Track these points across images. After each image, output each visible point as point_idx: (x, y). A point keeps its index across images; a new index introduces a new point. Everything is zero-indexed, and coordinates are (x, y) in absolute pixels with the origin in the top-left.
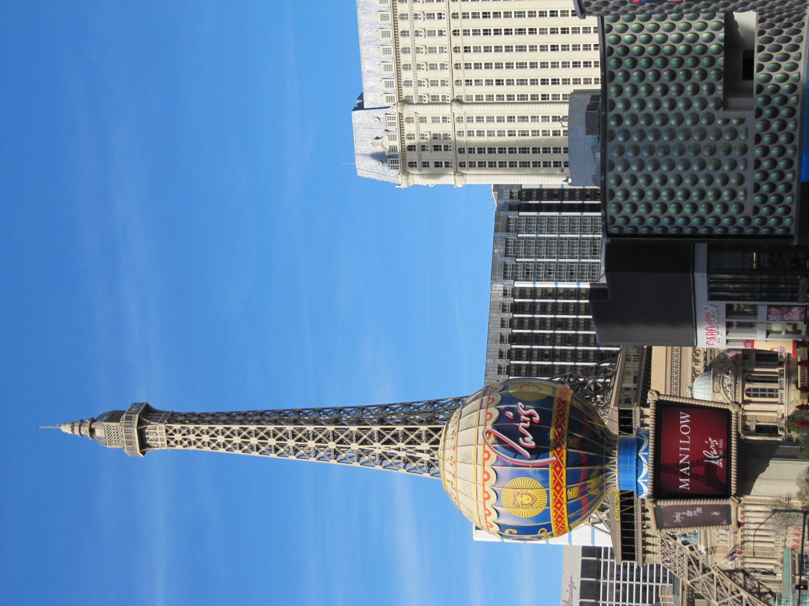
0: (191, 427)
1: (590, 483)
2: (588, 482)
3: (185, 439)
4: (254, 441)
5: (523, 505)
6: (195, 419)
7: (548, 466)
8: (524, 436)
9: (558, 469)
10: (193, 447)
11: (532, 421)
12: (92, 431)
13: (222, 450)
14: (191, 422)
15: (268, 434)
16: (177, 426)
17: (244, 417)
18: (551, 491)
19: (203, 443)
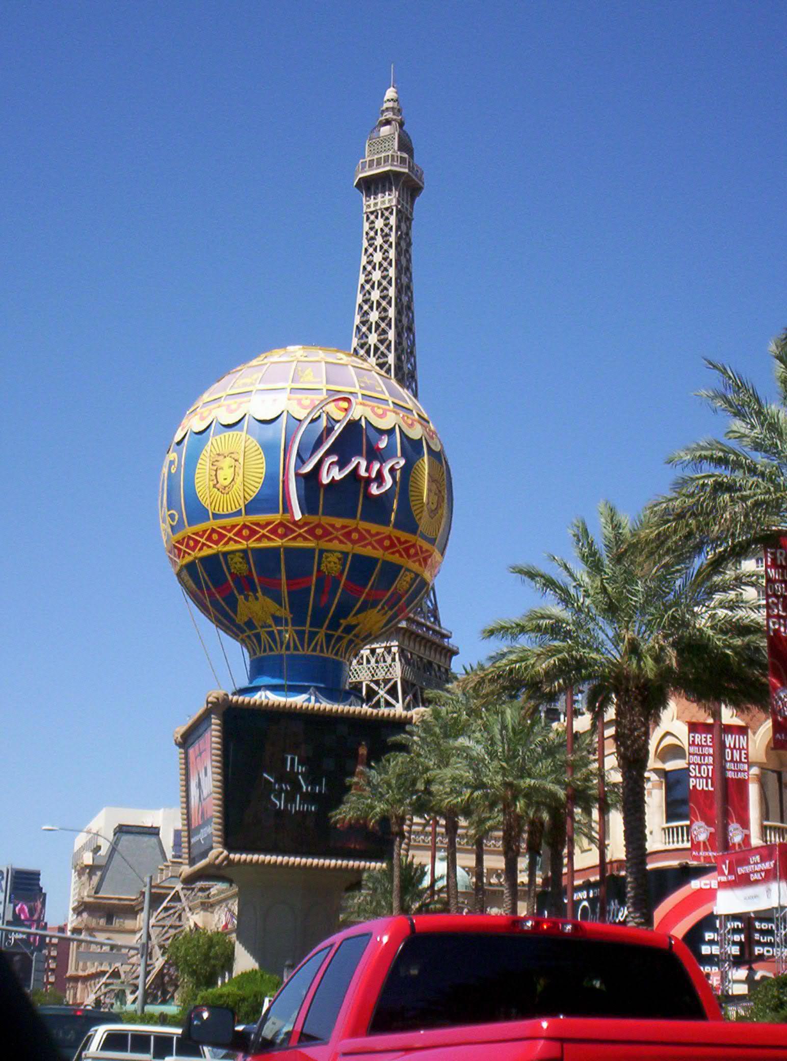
0: (392, 239)
1: (257, 599)
2: (259, 594)
3: (376, 233)
4: (374, 316)
5: (216, 471)
6: (403, 244)
7: (285, 511)
8: (342, 464)
9: (280, 531)
10: (365, 244)
11: (368, 481)
12: (388, 122)
13: (362, 278)
14: (399, 239)
15: (384, 332)
16: (393, 221)
17: (405, 309)
18: (240, 520)
19: (371, 255)
